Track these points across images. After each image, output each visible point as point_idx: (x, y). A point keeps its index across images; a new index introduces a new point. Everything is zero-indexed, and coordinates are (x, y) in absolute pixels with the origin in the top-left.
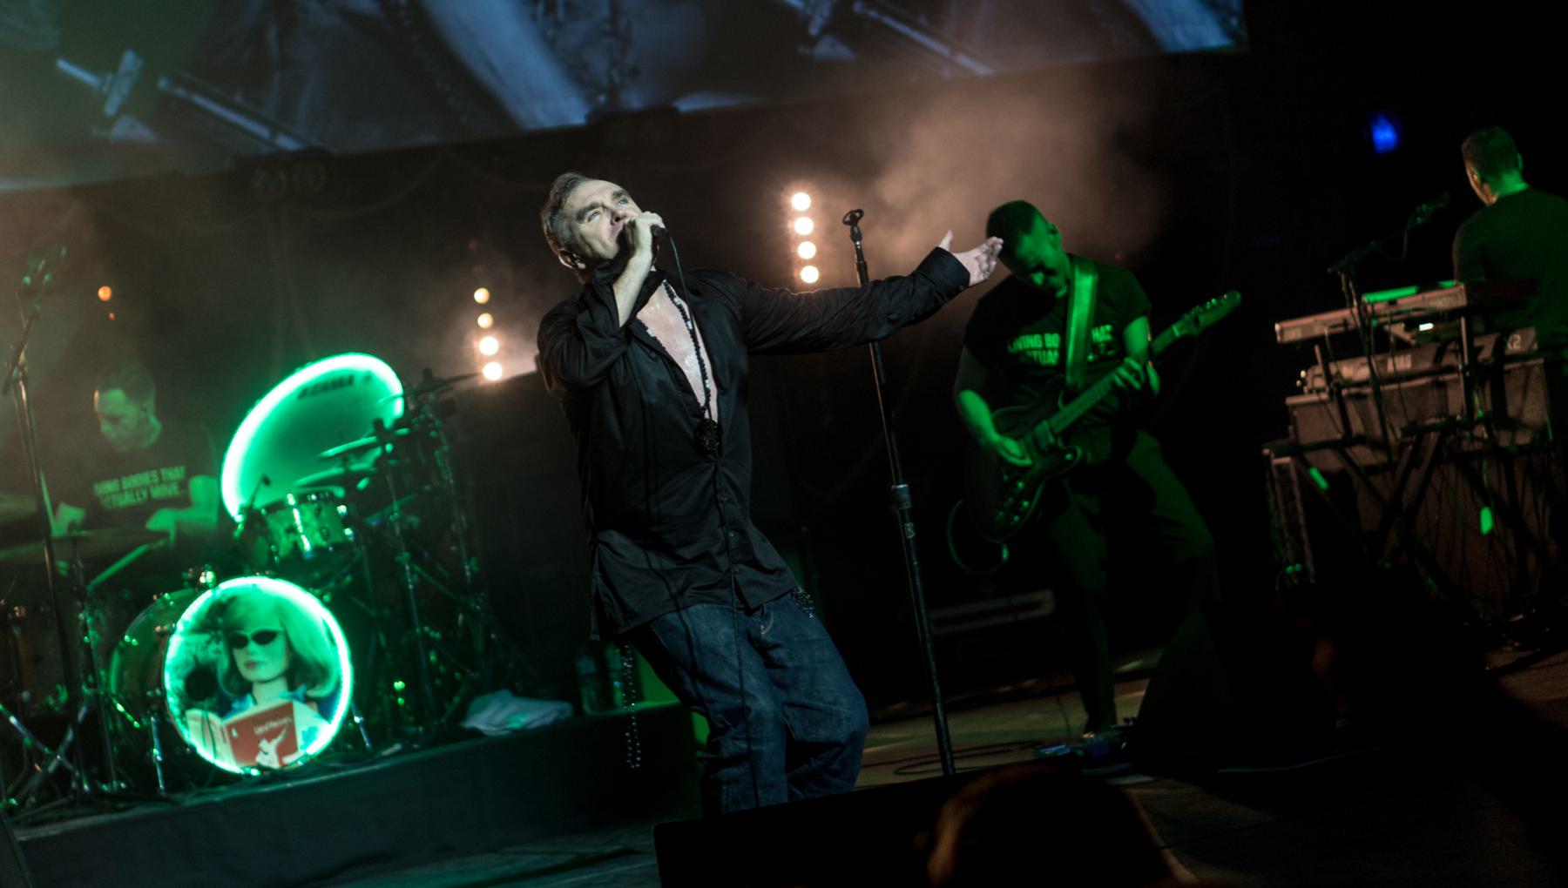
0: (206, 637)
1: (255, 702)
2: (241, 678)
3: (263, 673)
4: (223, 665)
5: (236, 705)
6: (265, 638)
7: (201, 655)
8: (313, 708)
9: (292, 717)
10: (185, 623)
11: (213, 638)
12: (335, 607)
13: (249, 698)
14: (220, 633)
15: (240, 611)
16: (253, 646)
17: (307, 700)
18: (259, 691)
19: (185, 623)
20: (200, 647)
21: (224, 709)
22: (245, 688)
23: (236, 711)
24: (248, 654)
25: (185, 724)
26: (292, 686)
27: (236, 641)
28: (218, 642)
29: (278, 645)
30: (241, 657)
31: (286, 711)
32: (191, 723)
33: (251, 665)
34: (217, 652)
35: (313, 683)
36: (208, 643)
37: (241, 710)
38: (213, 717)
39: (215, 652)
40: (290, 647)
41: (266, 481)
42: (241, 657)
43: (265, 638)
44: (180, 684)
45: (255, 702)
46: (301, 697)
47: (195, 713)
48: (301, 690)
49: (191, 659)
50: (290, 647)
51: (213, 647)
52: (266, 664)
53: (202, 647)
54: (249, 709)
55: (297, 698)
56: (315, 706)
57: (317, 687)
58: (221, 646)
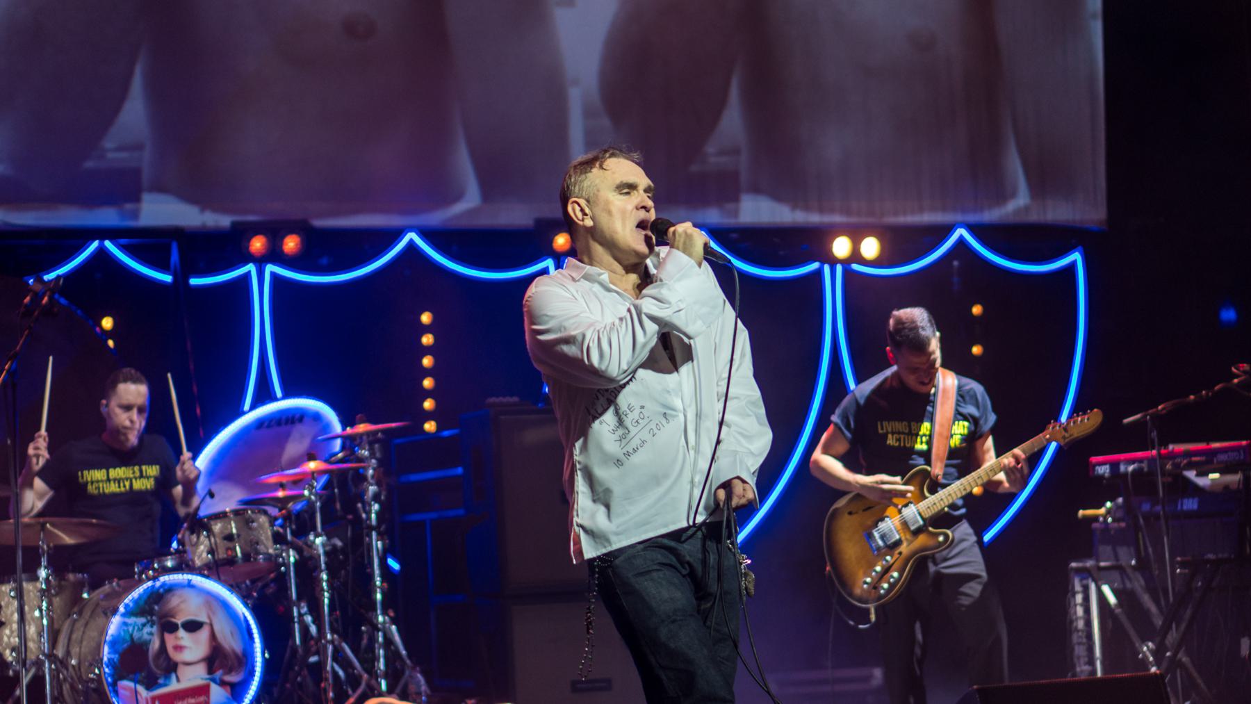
0: (142, 620)
1: (178, 680)
2: (168, 658)
3: (187, 656)
4: (156, 644)
5: (161, 681)
6: (193, 626)
7: (136, 635)
8: (226, 691)
9: (208, 697)
10: (126, 606)
11: (148, 622)
12: (255, 611)
13: (174, 677)
14: (154, 618)
15: (174, 601)
16: (181, 633)
17: (223, 684)
18: (182, 670)
19: (126, 606)
20: (136, 628)
21: (151, 684)
22: (171, 668)
23: (161, 686)
24: (177, 638)
25: (116, 693)
26: (211, 671)
27: (168, 627)
28: (152, 627)
29: (204, 634)
30: (170, 640)
31: (203, 690)
32: (121, 692)
33: (179, 648)
34: (151, 634)
35: (229, 671)
36: (144, 625)
37: (165, 685)
38: (140, 689)
39: (149, 634)
40: (213, 636)
41: (212, 495)
42: (170, 640)
43: (193, 626)
44: (116, 657)
45: (178, 680)
46: (218, 681)
47: (126, 684)
48: (218, 674)
49: (128, 638)
50: (213, 636)
51: (147, 629)
52: (192, 648)
53: (139, 628)
54: (173, 686)
55: (214, 680)
56: (228, 688)
57: (233, 673)
58: (155, 629)
